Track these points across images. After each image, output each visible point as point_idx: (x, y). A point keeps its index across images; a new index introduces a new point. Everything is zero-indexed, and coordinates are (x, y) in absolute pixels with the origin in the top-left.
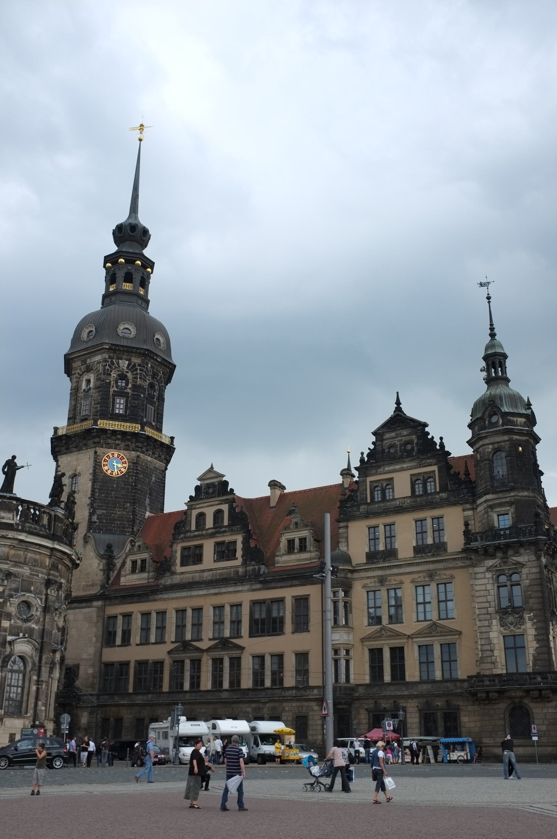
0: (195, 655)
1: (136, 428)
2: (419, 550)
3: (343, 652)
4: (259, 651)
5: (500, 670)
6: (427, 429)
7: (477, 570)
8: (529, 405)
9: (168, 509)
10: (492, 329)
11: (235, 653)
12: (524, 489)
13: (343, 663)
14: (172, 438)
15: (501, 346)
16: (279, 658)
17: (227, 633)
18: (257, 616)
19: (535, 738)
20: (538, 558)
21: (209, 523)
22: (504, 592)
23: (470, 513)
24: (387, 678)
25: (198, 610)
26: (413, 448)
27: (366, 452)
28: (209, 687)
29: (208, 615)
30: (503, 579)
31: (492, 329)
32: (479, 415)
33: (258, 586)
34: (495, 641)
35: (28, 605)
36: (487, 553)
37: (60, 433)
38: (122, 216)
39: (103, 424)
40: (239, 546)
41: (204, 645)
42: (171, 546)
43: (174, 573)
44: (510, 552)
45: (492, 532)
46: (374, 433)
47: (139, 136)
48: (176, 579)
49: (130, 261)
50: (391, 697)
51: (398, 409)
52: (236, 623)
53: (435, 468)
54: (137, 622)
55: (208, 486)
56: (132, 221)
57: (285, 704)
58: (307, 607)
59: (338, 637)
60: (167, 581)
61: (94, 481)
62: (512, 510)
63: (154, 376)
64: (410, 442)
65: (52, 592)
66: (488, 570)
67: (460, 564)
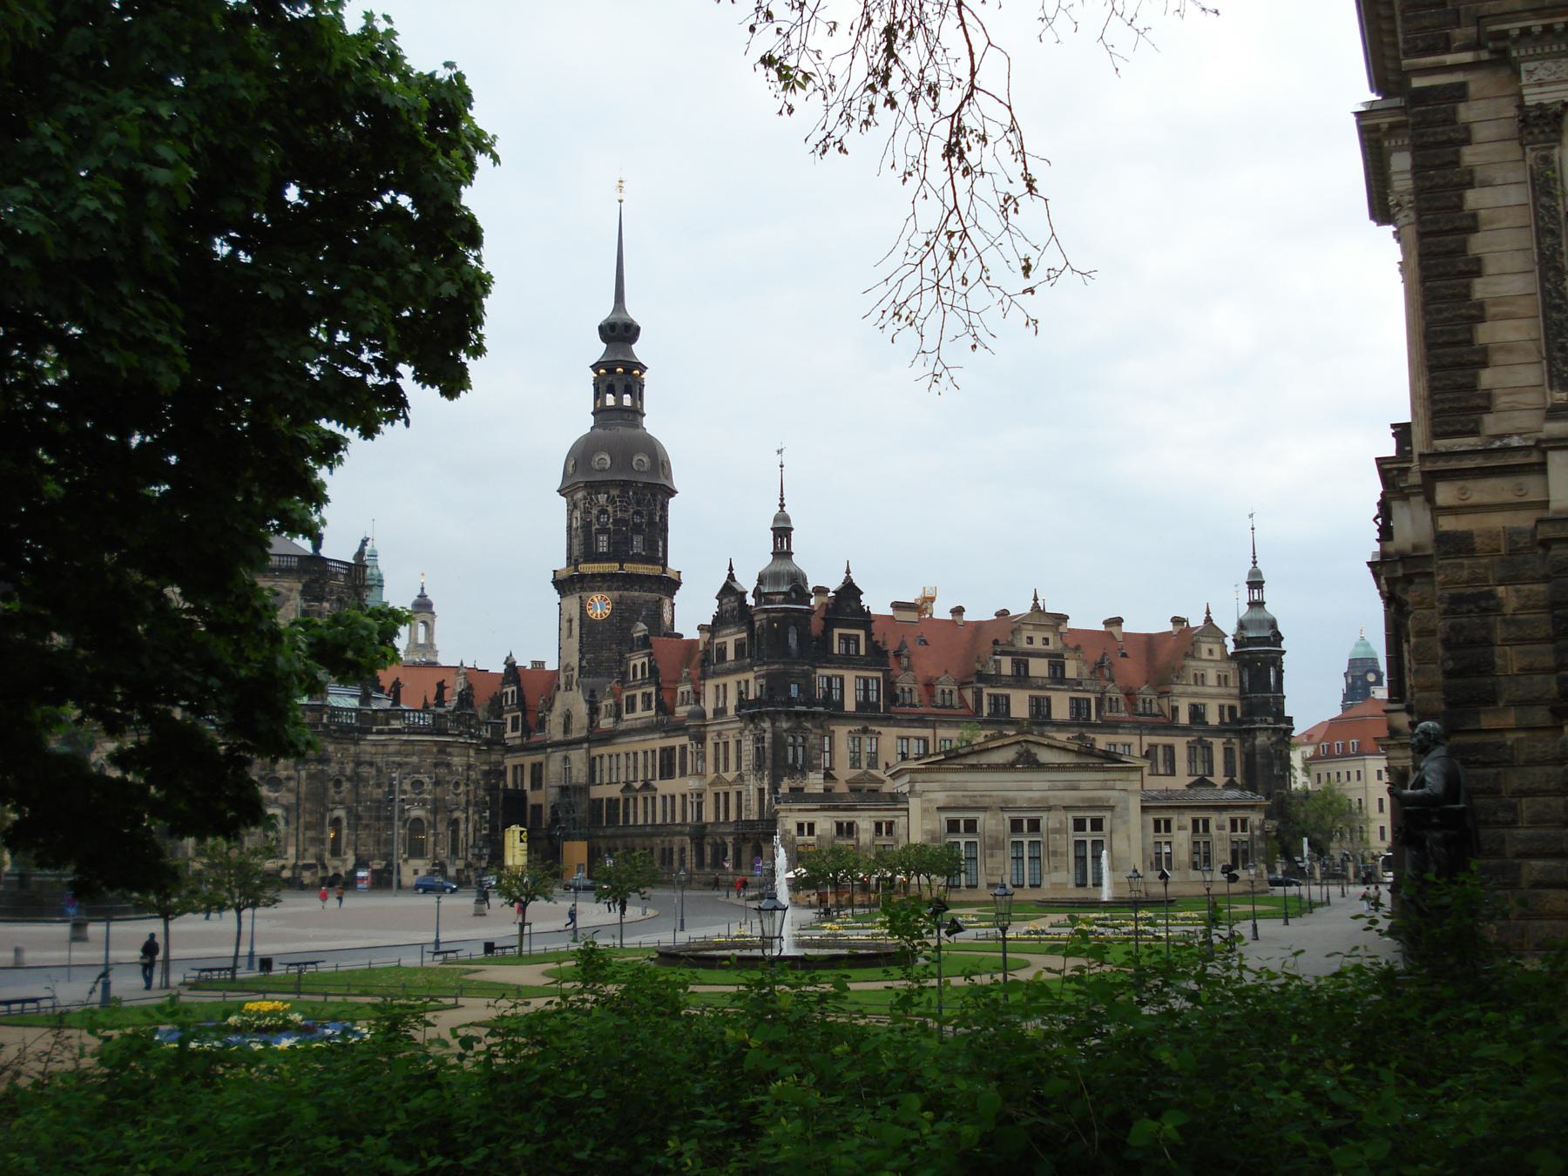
1: (613, 567)
2: (738, 709)
15: (787, 519)
20: (773, 724)
24: (722, 818)
25: (635, 754)
36: (752, 718)
38: (605, 311)
41: (638, 785)
49: (611, 371)
51: (731, 577)
52: (654, 766)
60: (622, 726)
62: (763, 681)
63: (638, 503)
65: (442, 771)
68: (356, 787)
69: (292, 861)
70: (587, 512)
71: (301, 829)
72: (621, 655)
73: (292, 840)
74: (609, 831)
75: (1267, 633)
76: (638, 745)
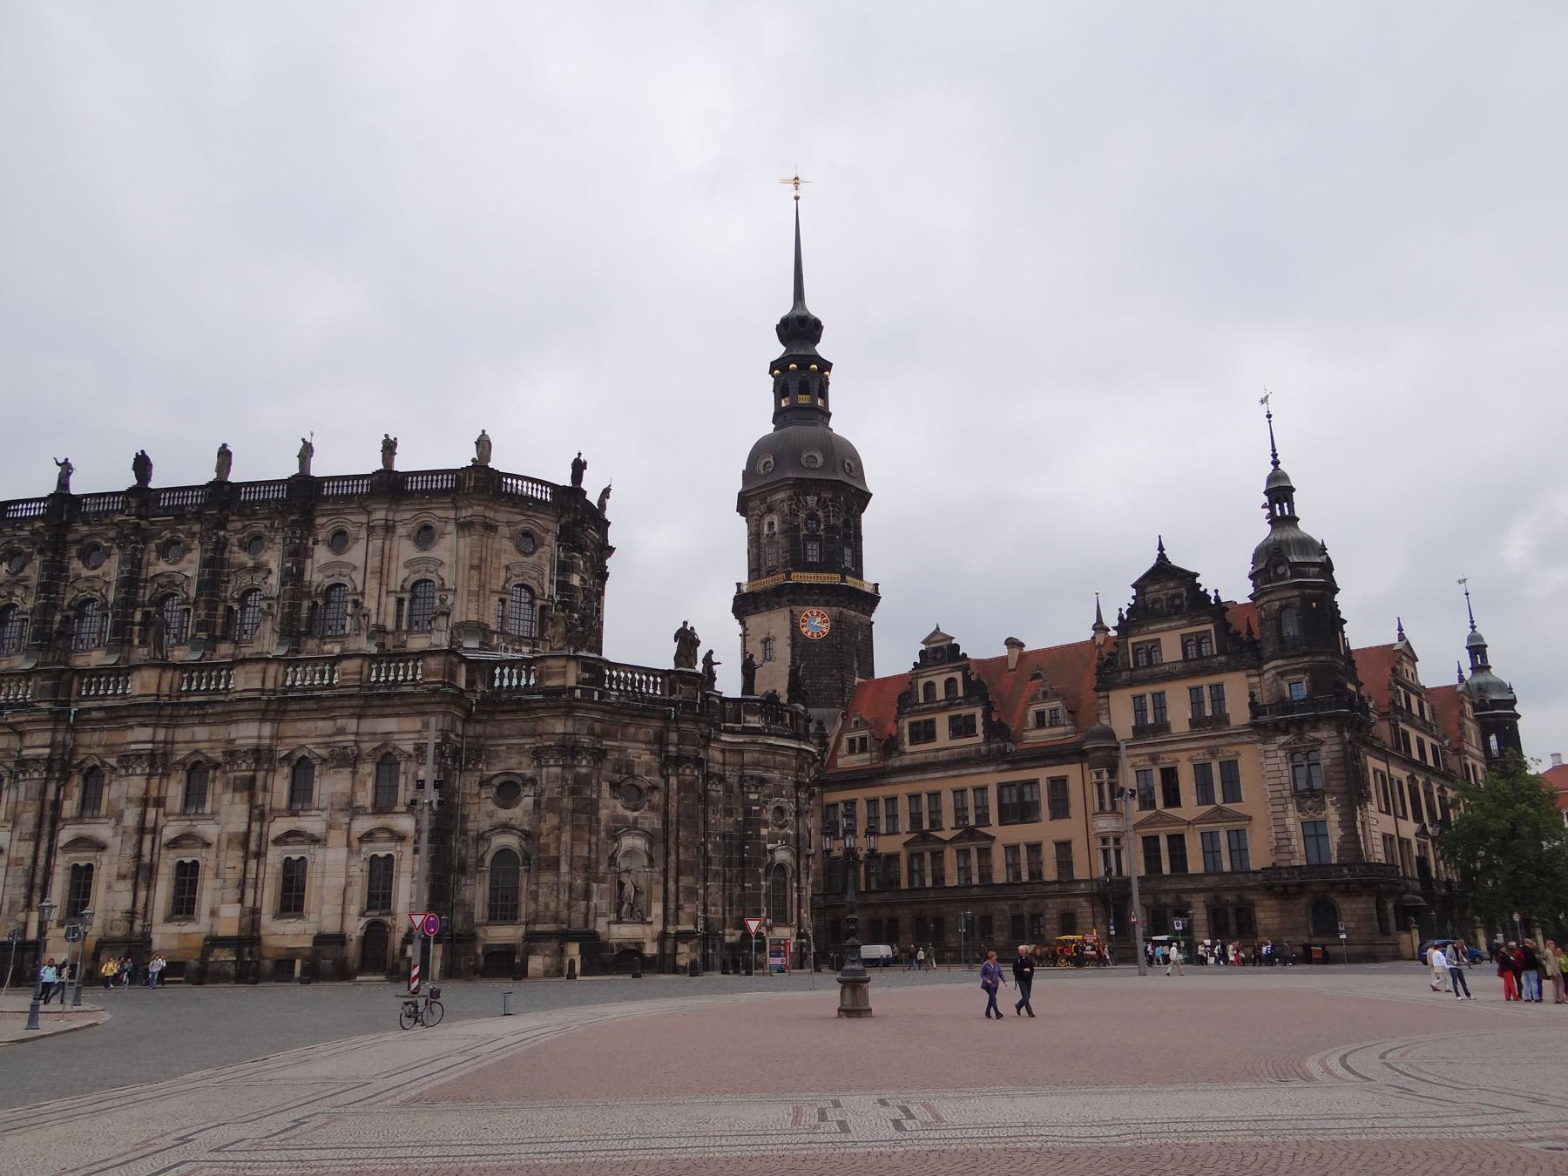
0: (937, 846)
2: (1197, 722)
3: (1111, 841)
4: (1012, 841)
5: (1300, 861)
6: (1198, 580)
7: (1267, 747)
8: (1323, 548)
9: (881, 672)
10: (1274, 455)
11: (983, 844)
12: (1320, 653)
13: (1112, 852)
14: (876, 585)
15: (1286, 477)
16: (1034, 848)
17: (972, 821)
18: (1006, 801)
19: (1343, 936)
20: (1340, 733)
21: (940, 694)
22: (1301, 773)
23: (1256, 679)
24: (1166, 869)
26: (1181, 605)
27: (1125, 608)
28: (956, 883)
29: (947, 802)
30: (1298, 757)
31: (1274, 455)
32: (1262, 566)
33: (1005, 767)
34: (1292, 828)
35: (780, 811)
36: (1278, 728)
37: (745, 589)
39: (800, 577)
40: (979, 721)
42: (896, 722)
43: (904, 753)
44: (1306, 727)
45: (1284, 705)
46: (1134, 586)
47: (794, 193)
48: (907, 760)
50: (1173, 891)
51: (1162, 557)
53: (1211, 627)
54: (862, 811)
55: (936, 650)
56: (798, 312)
57: (1050, 903)
58: (1065, 790)
59: (1105, 824)
60: (896, 762)
61: (793, 646)
63: (849, 509)
64: (1179, 596)
66: (1281, 747)
67: (1246, 739)
68: (705, 812)
69: (658, 927)
70: (794, 514)
71: (672, 873)
72: (843, 681)
73: (658, 891)
74: (873, 899)
75: (1509, 697)
76: (945, 784)
